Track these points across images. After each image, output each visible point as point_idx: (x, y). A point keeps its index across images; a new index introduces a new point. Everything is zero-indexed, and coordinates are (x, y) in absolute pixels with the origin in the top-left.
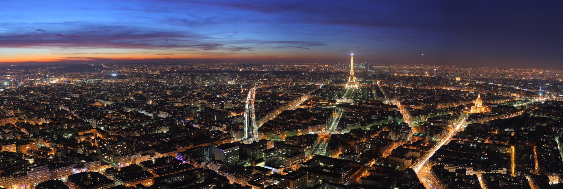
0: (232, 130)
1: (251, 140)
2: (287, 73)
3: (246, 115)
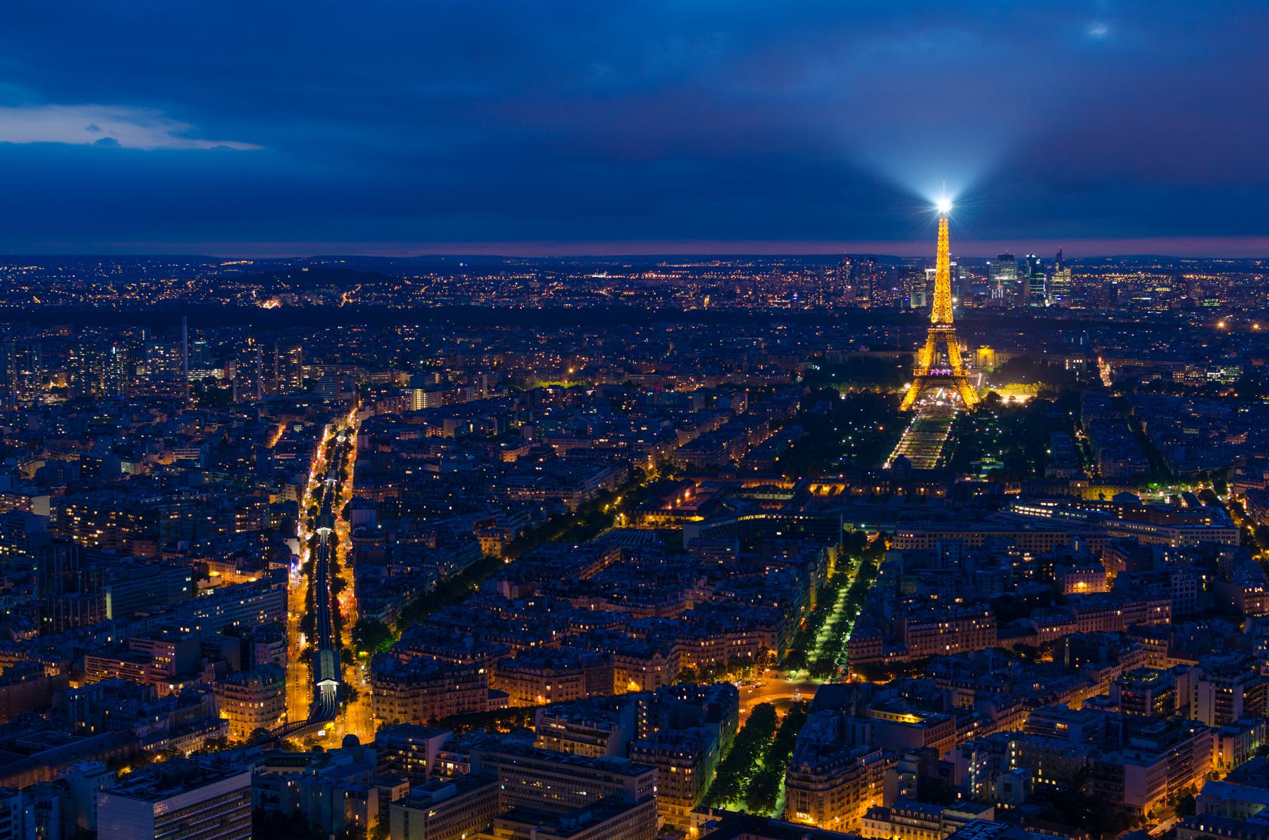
0: (209, 679)
1: (332, 734)
2: (551, 317)
3: (297, 580)
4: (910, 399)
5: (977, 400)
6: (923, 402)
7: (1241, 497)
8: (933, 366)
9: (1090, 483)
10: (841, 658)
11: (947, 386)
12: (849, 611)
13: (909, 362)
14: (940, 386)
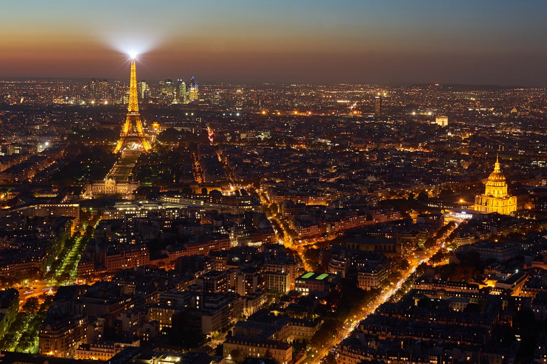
4: (119, 147)
5: (150, 148)
6: (125, 149)
7: (265, 190)
8: (129, 132)
9: (199, 186)
10: (73, 274)
11: (137, 142)
12: (79, 250)
13: (119, 129)
14: (134, 141)
